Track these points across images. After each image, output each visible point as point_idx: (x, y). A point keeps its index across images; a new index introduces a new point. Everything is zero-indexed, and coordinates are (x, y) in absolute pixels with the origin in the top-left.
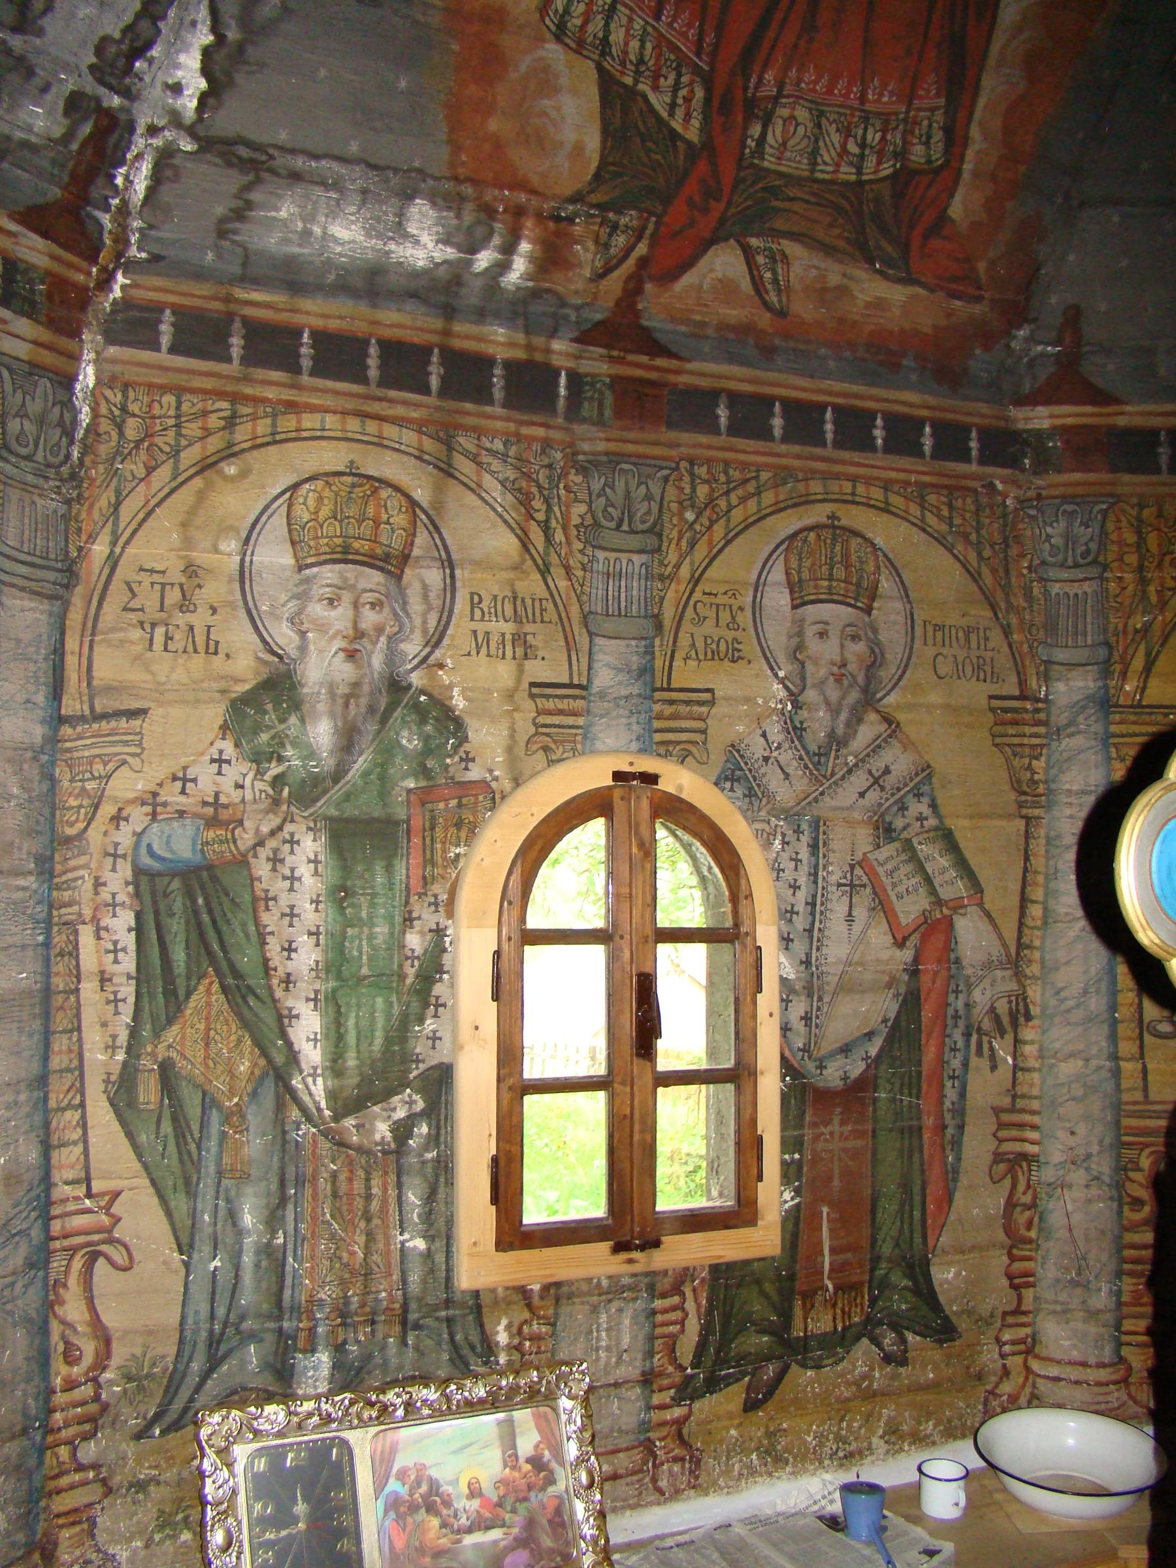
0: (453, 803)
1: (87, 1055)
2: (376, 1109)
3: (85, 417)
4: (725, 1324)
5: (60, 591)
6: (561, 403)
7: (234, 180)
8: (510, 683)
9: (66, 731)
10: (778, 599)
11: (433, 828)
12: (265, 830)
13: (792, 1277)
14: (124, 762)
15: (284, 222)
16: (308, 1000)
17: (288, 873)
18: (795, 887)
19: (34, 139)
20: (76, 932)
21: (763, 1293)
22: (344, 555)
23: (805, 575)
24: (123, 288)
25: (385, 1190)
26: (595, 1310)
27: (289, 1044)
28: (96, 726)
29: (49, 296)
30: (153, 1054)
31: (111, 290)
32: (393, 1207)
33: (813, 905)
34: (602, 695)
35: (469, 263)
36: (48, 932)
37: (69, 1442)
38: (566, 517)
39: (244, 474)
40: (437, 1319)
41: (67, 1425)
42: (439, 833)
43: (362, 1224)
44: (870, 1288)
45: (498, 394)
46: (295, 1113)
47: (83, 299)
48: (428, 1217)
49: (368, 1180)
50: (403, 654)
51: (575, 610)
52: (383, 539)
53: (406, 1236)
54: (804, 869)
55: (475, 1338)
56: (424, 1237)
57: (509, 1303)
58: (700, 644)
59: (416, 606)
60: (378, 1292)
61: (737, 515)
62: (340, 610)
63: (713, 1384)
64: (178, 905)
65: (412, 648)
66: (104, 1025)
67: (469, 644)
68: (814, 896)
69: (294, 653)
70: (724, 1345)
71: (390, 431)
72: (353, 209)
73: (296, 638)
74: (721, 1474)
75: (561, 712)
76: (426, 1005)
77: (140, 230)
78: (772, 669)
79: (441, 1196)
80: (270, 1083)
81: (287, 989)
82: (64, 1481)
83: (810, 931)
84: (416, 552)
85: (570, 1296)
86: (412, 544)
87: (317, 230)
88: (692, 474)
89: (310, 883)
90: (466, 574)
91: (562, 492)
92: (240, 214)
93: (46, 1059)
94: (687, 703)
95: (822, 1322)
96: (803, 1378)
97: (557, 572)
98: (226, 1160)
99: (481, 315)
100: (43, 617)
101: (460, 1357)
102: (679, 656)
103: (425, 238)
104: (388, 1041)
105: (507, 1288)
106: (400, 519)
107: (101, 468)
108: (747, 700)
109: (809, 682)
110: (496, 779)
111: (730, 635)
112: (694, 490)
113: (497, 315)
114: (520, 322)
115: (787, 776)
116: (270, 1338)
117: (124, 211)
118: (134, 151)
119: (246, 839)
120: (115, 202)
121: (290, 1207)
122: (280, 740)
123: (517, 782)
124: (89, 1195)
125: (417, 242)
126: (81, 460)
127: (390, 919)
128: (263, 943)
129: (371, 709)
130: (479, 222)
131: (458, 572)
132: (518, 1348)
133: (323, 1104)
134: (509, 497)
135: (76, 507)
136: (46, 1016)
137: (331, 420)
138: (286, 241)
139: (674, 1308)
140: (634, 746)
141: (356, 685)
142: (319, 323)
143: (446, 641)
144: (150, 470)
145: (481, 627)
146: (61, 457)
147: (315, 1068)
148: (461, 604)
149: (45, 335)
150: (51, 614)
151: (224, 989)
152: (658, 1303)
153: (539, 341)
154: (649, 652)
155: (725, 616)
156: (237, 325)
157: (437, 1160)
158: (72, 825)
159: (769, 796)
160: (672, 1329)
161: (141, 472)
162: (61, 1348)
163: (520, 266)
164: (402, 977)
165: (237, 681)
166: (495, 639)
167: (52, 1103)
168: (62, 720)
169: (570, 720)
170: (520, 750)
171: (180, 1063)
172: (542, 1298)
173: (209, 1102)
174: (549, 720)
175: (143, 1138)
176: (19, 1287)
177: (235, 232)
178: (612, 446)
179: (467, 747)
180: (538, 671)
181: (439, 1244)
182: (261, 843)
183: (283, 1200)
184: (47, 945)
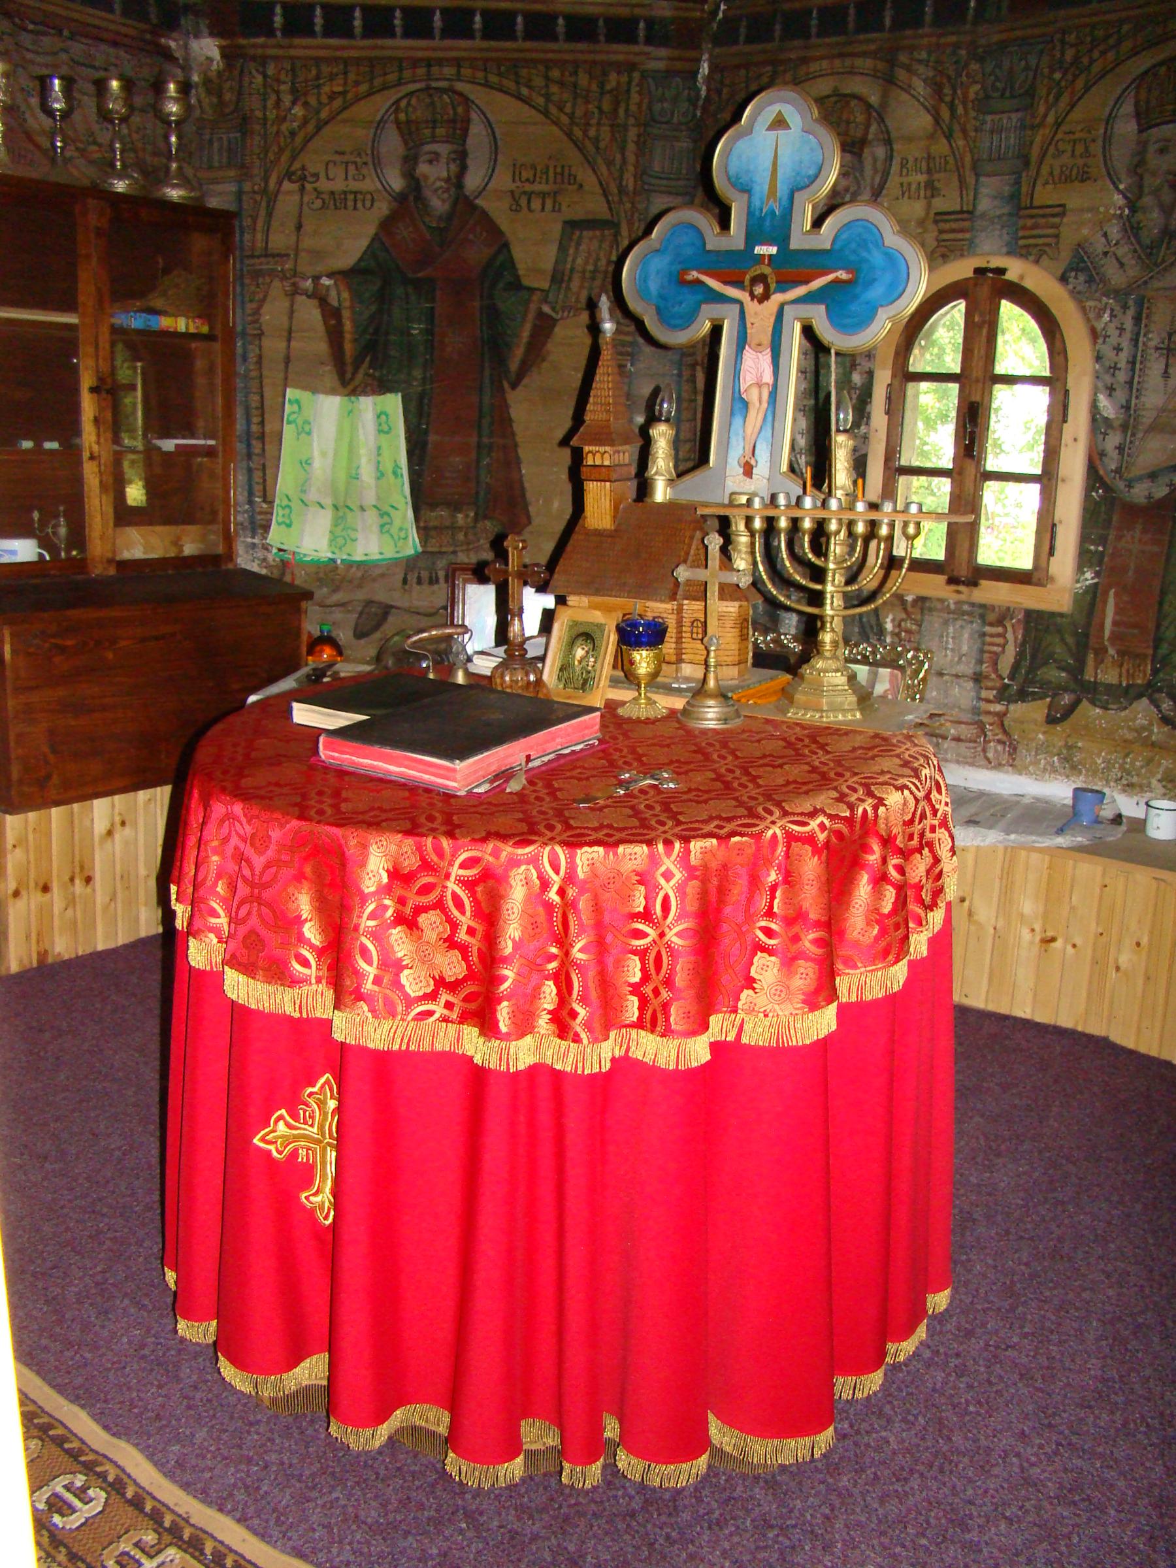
3: (703, 93)
4: (1034, 657)
10: (1127, 128)
13: (1086, 635)
18: (1118, 349)
21: (1063, 640)
23: (1154, 103)
26: (946, 623)
33: (1133, 363)
34: (983, 216)
38: (965, 95)
44: (1153, 661)
45: (928, 18)
51: (968, 159)
52: (852, 132)
54: (1128, 335)
58: (1057, 172)
61: (1096, 68)
63: (1023, 695)
68: (1135, 357)
70: (1032, 669)
71: (859, 62)
74: (1031, 763)
75: (953, 231)
78: (1114, 183)
83: (1130, 383)
84: (870, 137)
85: (930, 610)
88: (1063, 42)
94: (1044, 216)
95: (1109, 676)
96: (1090, 712)
97: (958, 134)
102: (1039, 183)
106: (860, 118)
108: (1093, 209)
109: (1146, 190)
111: (1080, 162)
112: (1063, 54)
115: (1122, 265)
131: (895, 147)
132: (898, 635)
134: (929, 90)
137: (825, 64)
139: (998, 635)
140: (1004, 250)
145: (905, 180)
148: (895, 167)
149: (676, 53)
152: (988, 629)
154: (1018, 183)
155: (1080, 149)
159: (1104, 280)
160: (995, 649)
166: (914, 187)
169: (960, 236)
178: (1004, 36)
180: (939, 204)
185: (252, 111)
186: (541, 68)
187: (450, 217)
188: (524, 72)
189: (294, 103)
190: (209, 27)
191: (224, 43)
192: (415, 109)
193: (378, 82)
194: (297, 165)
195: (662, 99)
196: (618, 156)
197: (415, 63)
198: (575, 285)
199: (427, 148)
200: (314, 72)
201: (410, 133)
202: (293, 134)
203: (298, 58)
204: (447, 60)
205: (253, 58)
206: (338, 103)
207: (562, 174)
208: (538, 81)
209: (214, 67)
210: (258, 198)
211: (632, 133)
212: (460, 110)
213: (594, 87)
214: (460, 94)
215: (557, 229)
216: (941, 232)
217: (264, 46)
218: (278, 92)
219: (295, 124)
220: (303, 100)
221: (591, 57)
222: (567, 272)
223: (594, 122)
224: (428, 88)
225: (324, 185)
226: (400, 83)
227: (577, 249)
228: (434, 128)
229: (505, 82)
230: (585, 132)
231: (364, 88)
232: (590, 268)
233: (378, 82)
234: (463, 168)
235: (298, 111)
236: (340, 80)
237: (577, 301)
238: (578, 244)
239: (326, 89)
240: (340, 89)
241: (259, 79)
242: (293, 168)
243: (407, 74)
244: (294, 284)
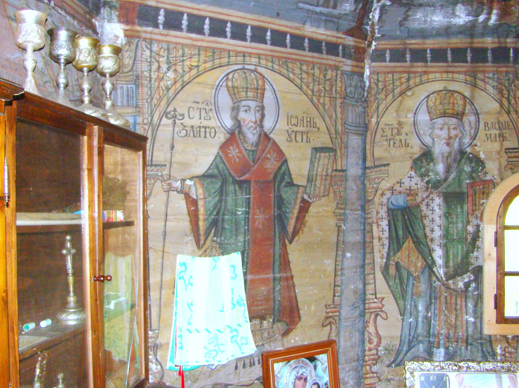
0: (481, 187)
1: (375, 260)
2: (459, 278)
3: (367, 84)
5: (364, 133)
6: (511, 59)
7: (403, 10)
8: (499, 149)
9: (368, 171)
11: (475, 194)
12: (424, 196)
14: (384, 179)
15: (418, 19)
16: (438, 245)
17: (431, 209)
19: (347, 12)
20: (372, 226)
22: (444, 115)
24: (375, 45)
25: (461, 302)
27: (432, 258)
28: (375, 169)
29: (355, 52)
30: (394, 260)
31: (371, 47)
32: (464, 308)
35: (477, 20)
36: (364, 226)
37: (370, 365)
39: (413, 94)
40: (478, 343)
41: (369, 360)
42: (477, 196)
43: (454, 312)
45: (490, 59)
46: (434, 278)
47: (364, 51)
48: (475, 312)
49: (456, 299)
50: (464, 143)
52: (456, 108)
53: (468, 317)
55: (489, 350)
56: (473, 317)
57: (501, 341)
59: (467, 127)
60: (459, 333)
62: (444, 131)
64: (400, 218)
65: (467, 140)
66: (380, 251)
67: (485, 138)
69: (431, 145)
71: (456, 76)
72: (439, 11)
73: (431, 140)
76: (474, 247)
77: (378, 28)
79: (479, 305)
80: (427, 269)
81: (432, 242)
82: (368, 376)
84: (466, 111)
86: (465, 109)
87: (429, 19)
89: (438, 212)
90: (483, 117)
91: (513, 87)
92: (405, 19)
93: (364, 261)
98: (414, 291)
99: (483, 35)
100: (360, 141)
101: (485, 356)
103: (462, 15)
104: (462, 259)
105: (500, 336)
106: (461, 102)
107: (373, 97)
110: (495, 179)
113: (488, 34)
114: (495, 35)
116: (426, 343)
117: (373, 24)
118: (374, 8)
119: (419, 199)
120: (370, 23)
121: (433, 305)
122: (428, 171)
123: (502, 179)
124: (376, 298)
125: (459, 17)
126: (367, 96)
127: (463, 222)
128: (424, 229)
129: (455, 160)
130: (478, 7)
131: (480, 116)
132: (504, 355)
133: (443, 276)
134: (495, 91)
135: (367, 109)
136: (364, 249)
137: (438, 75)
138: (420, 24)
141: (450, 153)
142: (431, 46)
143: (477, 138)
144: (386, 96)
145: (488, 132)
146: (362, 96)
147: (440, 266)
148: (482, 126)
149: (355, 63)
150: (362, 139)
151: (414, 242)
153: (502, 40)
156: (408, 51)
157: (478, 295)
158: (370, 196)
161: (384, 97)
162: (368, 339)
163: (494, 18)
164: (466, 239)
165: (414, 154)
167: (366, 272)
168: (366, 168)
170: (503, 169)
171: (401, 263)
172: (512, 340)
173: (409, 274)
174: (511, 160)
175: (391, 283)
176: (357, 321)
177: (404, 24)
179: (485, 169)
180: (508, 144)
181: (478, 320)
182: (423, 200)
183: (431, 303)
184: (364, 229)
185: (142, 72)
186: (298, 64)
187: (257, 144)
188: (290, 65)
189: (168, 69)
190: (119, 16)
192: (237, 80)
193: (217, 62)
194: (171, 108)
195: (350, 86)
196: (334, 114)
197: (237, 53)
198: (318, 183)
199: (244, 103)
200: (181, 52)
201: (234, 94)
202: (168, 89)
203: (172, 43)
204: (253, 53)
205: (145, 39)
206: (194, 72)
207: (310, 122)
208: (297, 71)
210: (146, 127)
211: (339, 101)
212: (260, 83)
213: (322, 77)
214: (260, 74)
215: (309, 153)
216: (509, 157)
217: (151, 33)
218: (158, 62)
219: (169, 83)
220: (173, 68)
221: (320, 61)
222: (314, 176)
223: (322, 95)
224: (243, 69)
225: (187, 121)
226: (228, 64)
227: (318, 163)
228: (247, 92)
229: (282, 69)
230: (318, 100)
231: (209, 65)
232: (324, 173)
233: (217, 62)
234: (263, 116)
235: (171, 74)
236: (195, 59)
237: (320, 192)
238: (319, 161)
240: (196, 64)
241: (148, 53)
242: (168, 110)
243: (233, 59)
244: (169, 184)
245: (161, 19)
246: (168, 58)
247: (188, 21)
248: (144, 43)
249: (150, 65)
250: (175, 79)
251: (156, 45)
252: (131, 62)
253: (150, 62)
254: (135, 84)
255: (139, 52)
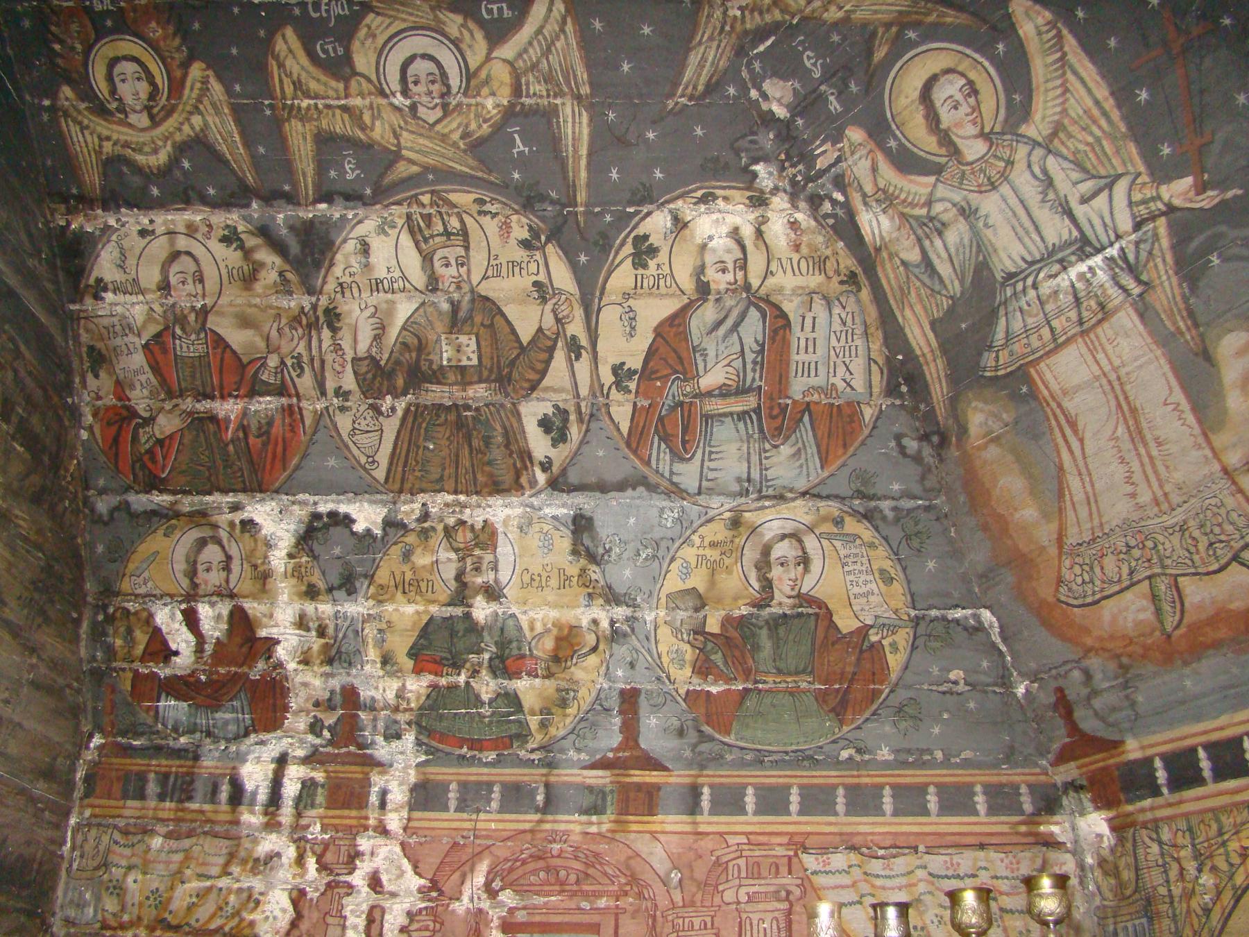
185: (1154, 888)
189: (1200, 870)
190: (1094, 801)
191: (1111, 814)
200: (1215, 826)
202: (1207, 911)
205: (1144, 825)
209: (1105, 844)
217: (1152, 809)
218: (1178, 860)
220: (1209, 864)
235: (1207, 879)
239: (1234, 845)
241: (1155, 848)
245: (1161, 775)
246: (1193, 845)
247: (1209, 758)
248: (1144, 832)
249: (1165, 872)
250: (1217, 886)
251: (1166, 829)
252: (1133, 875)
253: (1164, 866)
254: (1146, 916)
255: (1140, 851)
